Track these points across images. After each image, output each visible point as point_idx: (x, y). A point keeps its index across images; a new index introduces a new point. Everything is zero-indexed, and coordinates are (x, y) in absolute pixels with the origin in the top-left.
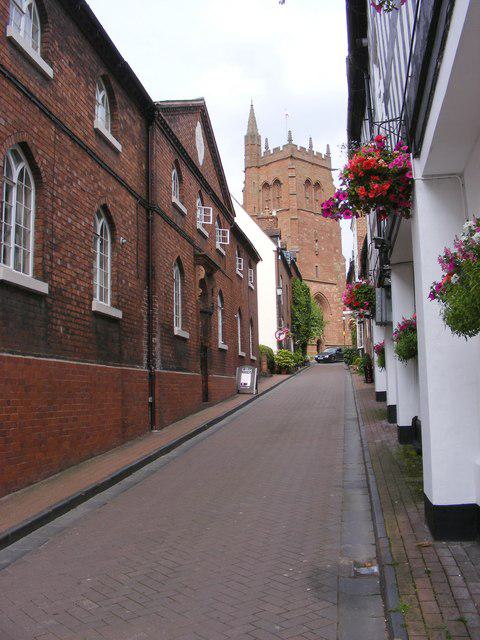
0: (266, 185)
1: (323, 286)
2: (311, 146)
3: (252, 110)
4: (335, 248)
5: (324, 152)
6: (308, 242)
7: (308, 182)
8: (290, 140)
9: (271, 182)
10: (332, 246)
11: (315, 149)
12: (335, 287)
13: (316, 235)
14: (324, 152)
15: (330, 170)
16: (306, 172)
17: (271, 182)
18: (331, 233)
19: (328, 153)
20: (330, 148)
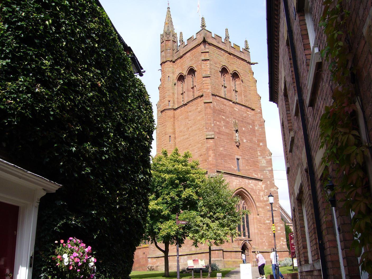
0: (181, 78)
1: (247, 181)
2: (227, 37)
4: (259, 141)
5: (242, 46)
6: (227, 131)
7: (224, 71)
8: (203, 26)
9: (185, 73)
10: (255, 139)
11: (234, 40)
12: (260, 183)
13: (235, 124)
14: (242, 46)
15: (249, 63)
16: (224, 60)
17: (185, 73)
18: (254, 126)
19: (247, 49)
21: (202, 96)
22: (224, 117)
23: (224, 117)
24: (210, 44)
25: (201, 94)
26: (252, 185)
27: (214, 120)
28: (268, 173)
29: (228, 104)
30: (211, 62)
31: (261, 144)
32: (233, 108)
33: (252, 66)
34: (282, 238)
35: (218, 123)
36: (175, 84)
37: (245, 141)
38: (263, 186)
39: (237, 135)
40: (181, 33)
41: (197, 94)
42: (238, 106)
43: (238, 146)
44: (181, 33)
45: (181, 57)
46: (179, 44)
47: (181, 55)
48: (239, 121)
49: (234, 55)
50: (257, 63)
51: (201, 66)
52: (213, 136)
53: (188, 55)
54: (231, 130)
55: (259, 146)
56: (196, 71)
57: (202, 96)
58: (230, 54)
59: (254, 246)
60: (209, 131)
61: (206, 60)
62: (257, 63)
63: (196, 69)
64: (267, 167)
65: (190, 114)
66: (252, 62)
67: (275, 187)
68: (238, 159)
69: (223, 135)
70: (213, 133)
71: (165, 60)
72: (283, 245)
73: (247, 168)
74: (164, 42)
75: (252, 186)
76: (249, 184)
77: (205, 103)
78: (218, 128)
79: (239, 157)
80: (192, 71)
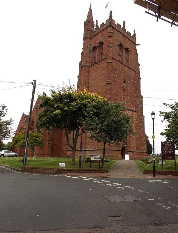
2: (124, 26)
3: (90, 8)
5: (132, 34)
7: (120, 45)
8: (111, 16)
9: (97, 45)
11: (127, 29)
12: (135, 113)
13: (124, 78)
14: (132, 34)
16: (121, 40)
17: (97, 45)
19: (134, 35)
20: (136, 33)
21: (106, 59)
22: (118, 73)
23: (118, 73)
24: (113, 27)
25: (105, 57)
26: (130, 114)
27: (112, 74)
28: (140, 108)
29: (121, 66)
30: (114, 39)
31: (137, 91)
32: (124, 68)
33: (137, 46)
34: (144, 145)
35: (114, 76)
36: (91, 52)
37: (128, 88)
38: (136, 115)
39: (124, 84)
40: (97, 21)
41: (104, 57)
42: (127, 68)
43: (124, 91)
44: (97, 21)
45: (96, 35)
46: (95, 27)
47: (96, 34)
48: (126, 76)
49: (127, 38)
50: (139, 45)
51: (107, 40)
52: (111, 82)
53: (100, 34)
54: (121, 81)
55: (136, 92)
56: (104, 44)
57: (106, 59)
58: (124, 36)
59: (128, 148)
60: (109, 79)
61: (110, 37)
62: (139, 45)
63: (103, 42)
64: (139, 105)
65: (98, 69)
66: (137, 43)
67: (143, 116)
68: (124, 98)
69: (117, 83)
70: (111, 81)
71: (86, 37)
72: (145, 149)
73: (128, 104)
74: (86, 26)
75: (130, 114)
76: (129, 113)
77: (107, 62)
78: (114, 79)
79: (123, 97)
80: (101, 44)
